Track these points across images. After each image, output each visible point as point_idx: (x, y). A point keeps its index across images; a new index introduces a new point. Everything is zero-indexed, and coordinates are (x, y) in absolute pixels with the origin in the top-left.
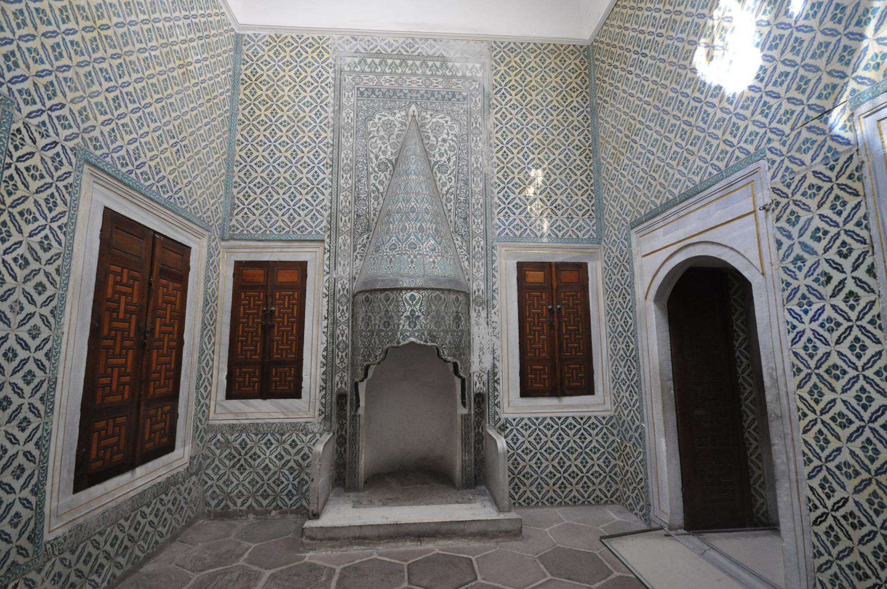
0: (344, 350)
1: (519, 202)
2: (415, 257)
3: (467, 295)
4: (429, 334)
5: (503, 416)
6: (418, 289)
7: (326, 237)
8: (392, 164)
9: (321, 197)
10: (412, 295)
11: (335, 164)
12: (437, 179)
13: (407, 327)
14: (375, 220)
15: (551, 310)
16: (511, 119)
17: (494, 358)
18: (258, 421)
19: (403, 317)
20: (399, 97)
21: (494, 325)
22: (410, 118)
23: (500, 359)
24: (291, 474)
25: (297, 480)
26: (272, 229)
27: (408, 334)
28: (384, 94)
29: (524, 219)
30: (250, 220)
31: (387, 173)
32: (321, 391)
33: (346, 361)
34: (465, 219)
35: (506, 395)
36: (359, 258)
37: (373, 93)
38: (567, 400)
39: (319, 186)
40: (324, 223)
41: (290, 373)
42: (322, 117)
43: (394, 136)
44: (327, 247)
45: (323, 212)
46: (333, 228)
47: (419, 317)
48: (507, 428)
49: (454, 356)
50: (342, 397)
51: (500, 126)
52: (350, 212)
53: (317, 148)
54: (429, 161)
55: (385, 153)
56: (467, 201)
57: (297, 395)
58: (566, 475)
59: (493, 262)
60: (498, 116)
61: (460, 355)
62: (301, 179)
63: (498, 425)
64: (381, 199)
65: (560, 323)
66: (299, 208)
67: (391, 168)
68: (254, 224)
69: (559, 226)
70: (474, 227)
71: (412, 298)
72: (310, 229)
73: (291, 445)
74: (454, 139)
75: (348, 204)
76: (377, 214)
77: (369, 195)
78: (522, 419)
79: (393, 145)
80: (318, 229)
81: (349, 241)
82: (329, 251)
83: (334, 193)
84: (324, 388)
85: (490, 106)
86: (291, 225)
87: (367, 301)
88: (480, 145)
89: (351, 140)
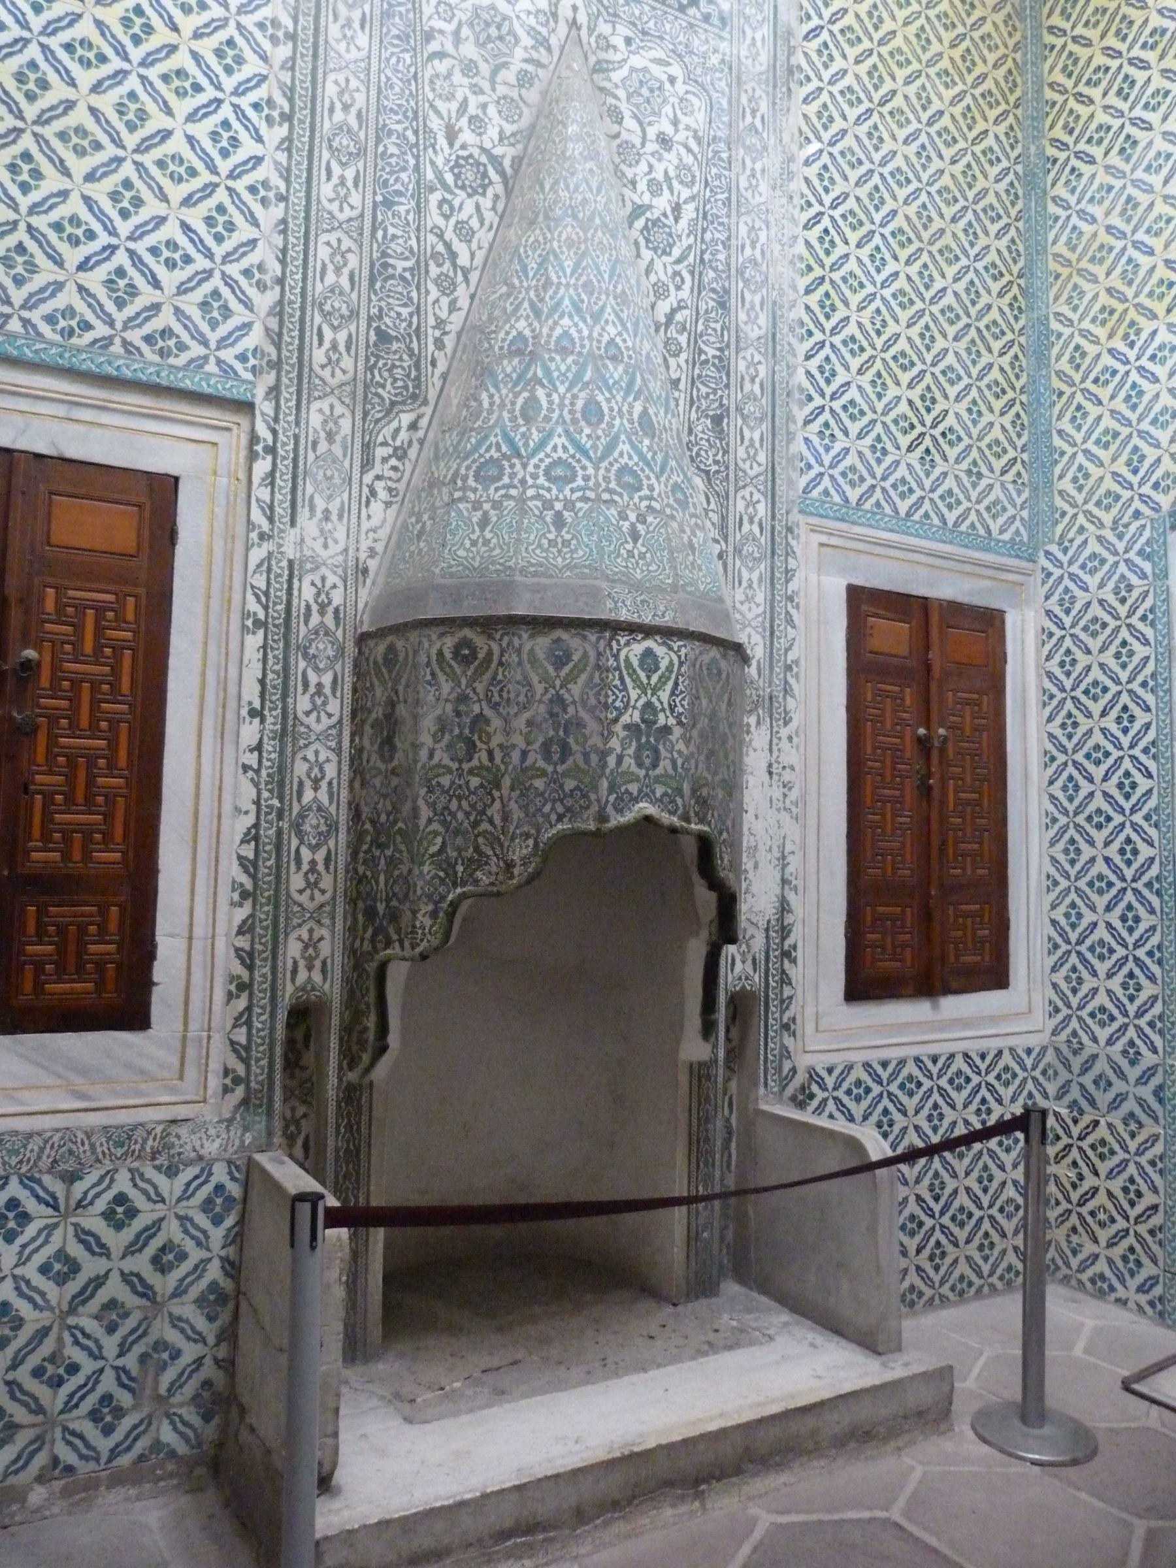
0: (323, 837)
2: (641, 519)
4: (694, 791)
5: (803, 1062)
6: (667, 633)
7: (260, 392)
8: (502, 173)
9: (245, 232)
10: (648, 653)
11: (302, 114)
13: (629, 762)
14: (442, 366)
15: (923, 744)
17: (784, 881)
19: (618, 728)
21: (787, 776)
23: (799, 883)
24: (111, 1329)
25: (138, 1350)
26: (35, 316)
27: (634, 788)
31: (486, 203)
32: (230, 996)
33: (327, 882)
34: (717, 420)
35: (810, 997)
36: (382, 494)
38: (954, 1006)
40: (254, 338)
41: (103, 928)
46: (288, 361)
47: (667, 729)
48: (812, 1096)
50: (303, 1016)
56: (723, 365)
57: (131, 1012)
59: (789, 574)
63: (790, 1091)
64: (462, 293)
65: (943, 781)
67: (499, 188)
70: (741, 453)
71: (649, 660)
72: (197, 350)
74: (693, 144)
75: (345, 282)
76: (450, 342)
80: (228, 355)
81: (346, 425)
82: (271, 450)
84: (242, 987)
85: (790, 72)
88: (763, 187)
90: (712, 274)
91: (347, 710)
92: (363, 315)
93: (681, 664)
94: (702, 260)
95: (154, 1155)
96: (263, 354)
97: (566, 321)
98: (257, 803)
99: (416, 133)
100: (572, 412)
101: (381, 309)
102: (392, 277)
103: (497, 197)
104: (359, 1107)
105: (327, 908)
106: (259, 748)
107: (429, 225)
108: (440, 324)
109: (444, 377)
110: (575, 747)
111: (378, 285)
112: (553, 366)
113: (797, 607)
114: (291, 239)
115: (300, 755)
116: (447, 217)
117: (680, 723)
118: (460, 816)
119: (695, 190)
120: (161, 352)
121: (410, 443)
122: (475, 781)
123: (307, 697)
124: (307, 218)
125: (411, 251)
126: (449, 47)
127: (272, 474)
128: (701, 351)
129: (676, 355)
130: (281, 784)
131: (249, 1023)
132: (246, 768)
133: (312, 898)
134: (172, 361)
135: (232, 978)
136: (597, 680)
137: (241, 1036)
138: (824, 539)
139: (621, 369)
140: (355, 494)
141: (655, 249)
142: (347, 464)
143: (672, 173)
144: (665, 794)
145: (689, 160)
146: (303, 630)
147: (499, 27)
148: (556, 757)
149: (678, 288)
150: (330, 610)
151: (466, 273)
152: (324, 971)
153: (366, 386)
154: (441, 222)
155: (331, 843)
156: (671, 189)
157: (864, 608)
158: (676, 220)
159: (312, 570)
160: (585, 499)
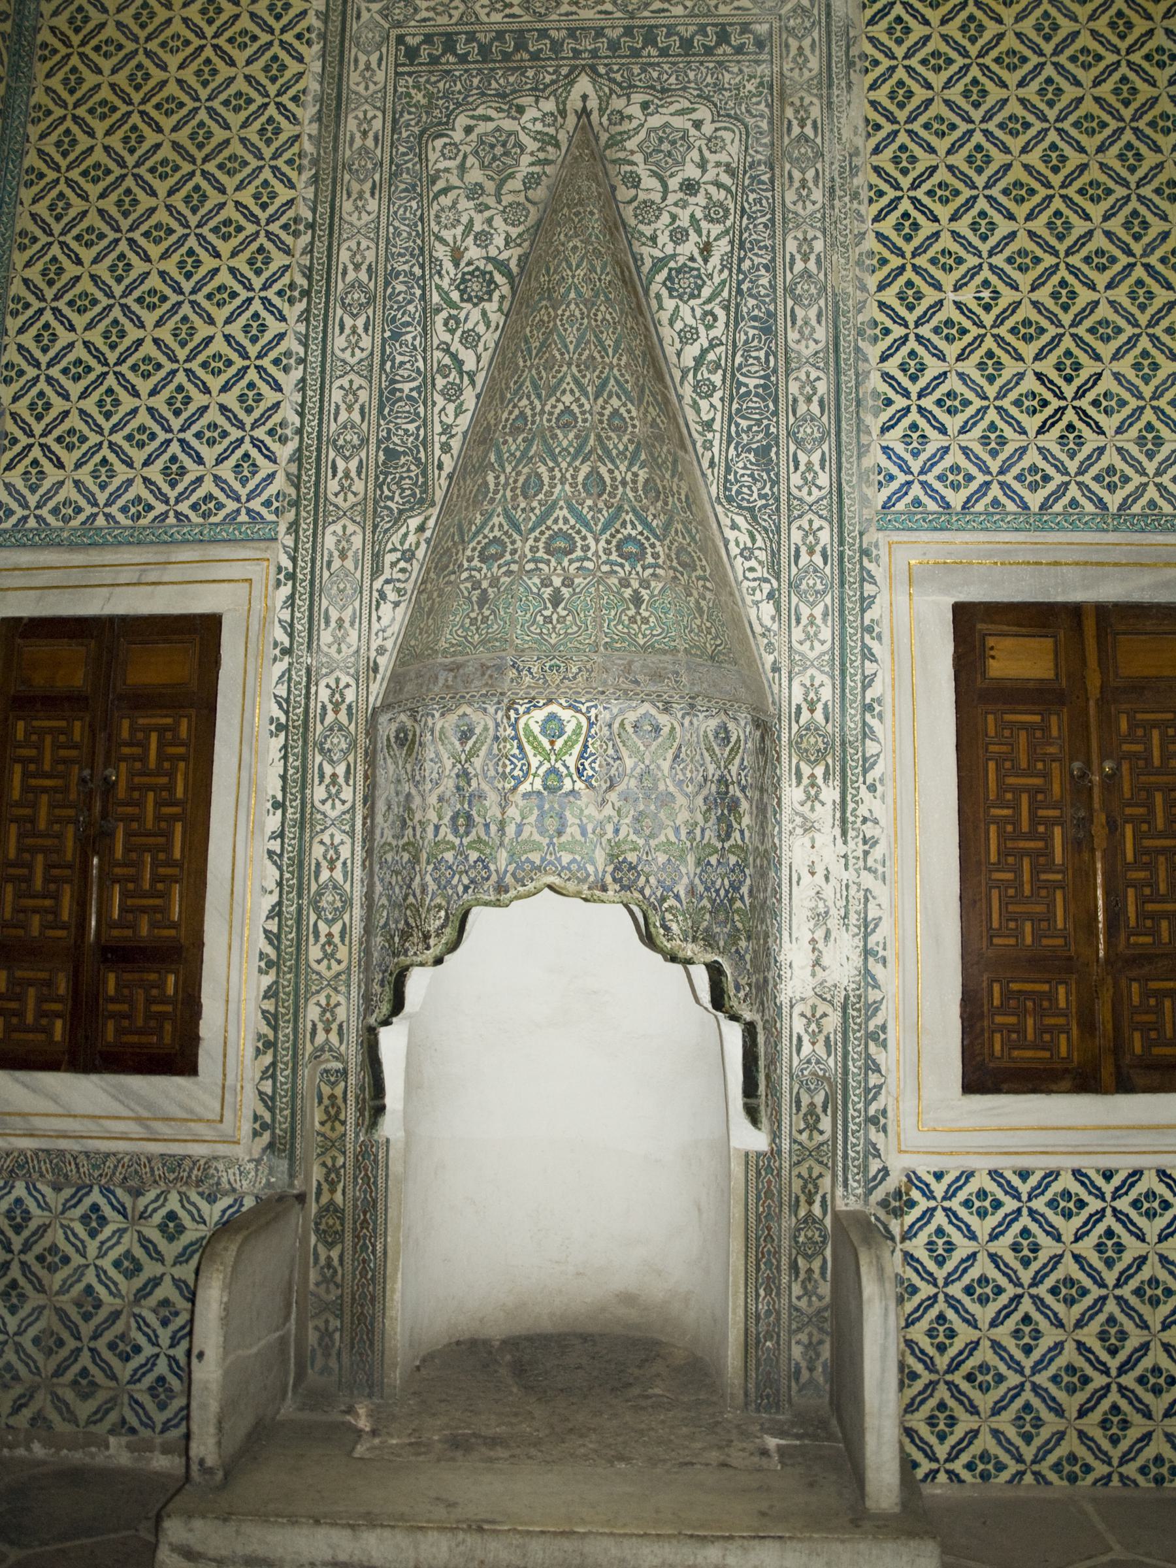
0: (338, 913)
1: (959, 388)
2: (568, 582)
4: (612, 857)
5: (898, 1164)
7: (282, 528)
8: (508, 274)
10: (552, 717)
12: (664, 317)
14: (448, 468)
16: (928, 102)
17: (867, 953)
18: (63, 1144)
19: (517, 798)
20: (535, 56)
21: (869, 830)
22: (571, 120)
23: (889, 954)
26: (114, 510)
27: (536, 858)
28: (485, 50)
29: (978, 449)
30: (47, 484)
31: (491, 307)
33: (342, 953)
34: (763, 453)
36: (392, 596)
37: (450, 47)
39: (266, 362)
40: (280, 483)
42: (283, 137)
43: (516, 184)
44: (286, 563)
45: (275, 446)
48: (912, 1204)
49: (709, 941)
51: (888, 128)
52: (364, 441)
53: (262, 239)
54: (638, 259)
55: (482, 239)
56: (769, 391)
58: (1128, 1380)
59: (866, 603)
61: (734, 937)
62: (209, 340)
63: (879, 1194)
64: (469, 398)
67: (506, 290)
68: (60, 497)
69: (1111, 470)
70: (796, 479)
72: (231, 506)
73: (163, 1228)
75: (356, 416)
76: (456, 444)
77: (427, 384)
78: (969, 1175)
79: (512, 213)
80: (255, 505)
81: (357, 541)
82: (292, 576)
84: (270, 1045)
85: (851, 64)
86: (172, 495)
87: (401, 742)
89: (372, 205)
90: (752, 302)
91: (359, 797)
92: (373, 439)
93: (591, 725)
94: (739, 292)
95: (199, 1182)
97: (525, 402)
98: (280, 884)
99: (422, 267)
103: (503, 297)
104: (376, 1161)
106: (282, 835)
107: (436, 342)
108: (447, 429)
109: (450, 477)
110: (477, 819)
112: (505, 448)
113: (879, 638)
116: (452, 332)
117: (590, 786)
119: (728, 223)
120: (204, 516)
121: (418, 544)
122: (406, 856)
124: (323, 372)
125: (418, 371)
127: (292, 597)
128: (740, 384)
129: (709, 396)
131: (273, 1077)
132: (270, 853)
133: (329, 968)
134: (213, 520)
135: (260, 1037)
137: (267, 1086)
139: (571, 436)
140: (366, 600)
142: (358, 575)
143: (699, 215)
144: (574, 861)
145: (719, 195)
146: (319, 728)
147: (504, 145)
148: (462, 830)
149: (709, 327)
150: (344, 707)
151: (471, 376)
153: (376, 502)
154: (447, 337)
155: (346, 917)
156: (699, 232)
157: (979, 626)
160: (509, 573)
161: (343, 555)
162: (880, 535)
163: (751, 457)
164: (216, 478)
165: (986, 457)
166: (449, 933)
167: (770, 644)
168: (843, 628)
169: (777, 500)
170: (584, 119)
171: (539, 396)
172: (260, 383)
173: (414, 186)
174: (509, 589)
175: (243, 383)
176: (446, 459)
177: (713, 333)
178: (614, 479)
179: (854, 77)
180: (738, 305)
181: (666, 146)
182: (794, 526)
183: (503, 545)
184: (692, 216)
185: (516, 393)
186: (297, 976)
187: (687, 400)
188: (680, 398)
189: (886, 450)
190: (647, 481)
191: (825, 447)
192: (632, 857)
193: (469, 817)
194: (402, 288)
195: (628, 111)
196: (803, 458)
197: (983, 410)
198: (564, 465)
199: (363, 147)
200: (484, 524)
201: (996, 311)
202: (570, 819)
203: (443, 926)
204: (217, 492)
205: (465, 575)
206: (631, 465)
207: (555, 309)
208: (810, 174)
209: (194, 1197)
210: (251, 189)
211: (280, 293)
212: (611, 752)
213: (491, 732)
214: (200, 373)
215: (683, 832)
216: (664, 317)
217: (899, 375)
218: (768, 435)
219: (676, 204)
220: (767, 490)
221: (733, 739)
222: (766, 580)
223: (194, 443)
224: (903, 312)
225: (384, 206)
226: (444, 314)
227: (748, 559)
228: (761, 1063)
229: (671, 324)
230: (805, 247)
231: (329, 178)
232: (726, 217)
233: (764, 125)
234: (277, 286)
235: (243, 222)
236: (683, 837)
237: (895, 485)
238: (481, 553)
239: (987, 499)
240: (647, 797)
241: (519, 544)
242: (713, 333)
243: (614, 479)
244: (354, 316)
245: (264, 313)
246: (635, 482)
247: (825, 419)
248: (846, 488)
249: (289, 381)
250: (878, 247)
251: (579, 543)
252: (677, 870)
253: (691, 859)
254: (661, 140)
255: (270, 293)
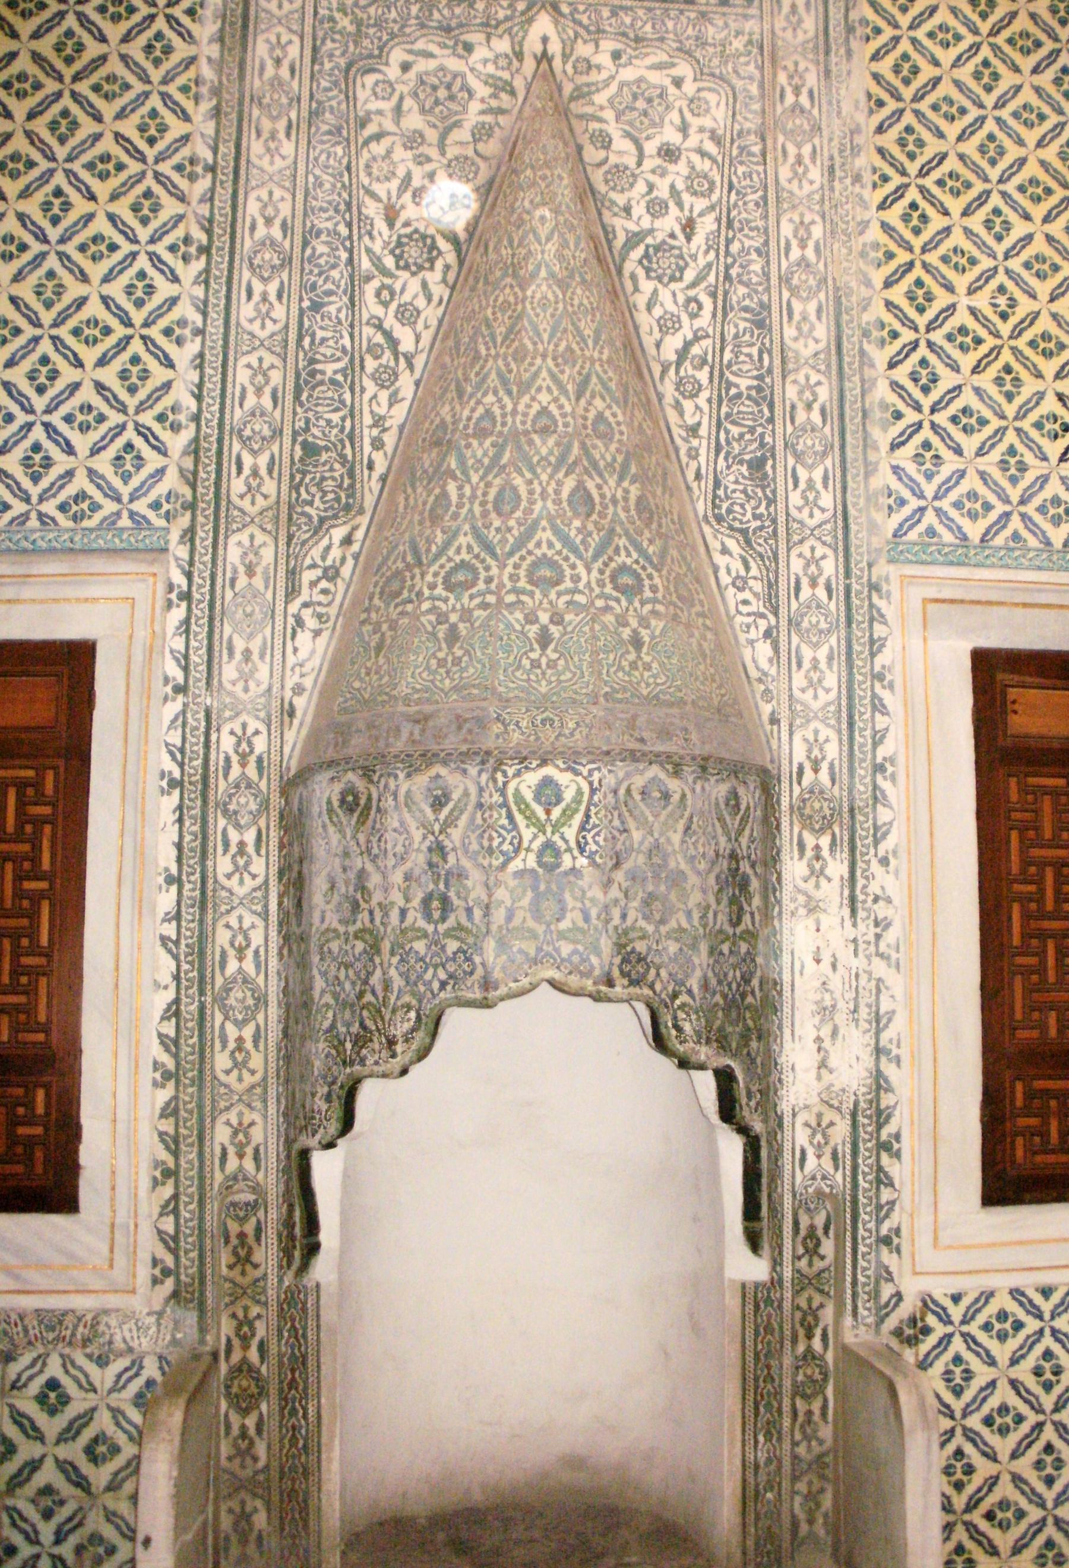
1: (975, 404)
2: (557, 619)
3: (768, 783)
4: (620, 946)
7: (174, 536)
10: (547, 782)
11: (222, 241)
12: (641, 300)
14: (380, 468)
17: (878, 1051)
21: (881, 910)
23: (904, 1052)
31: (433, 278)
33: (256, 1061)
34: (757, 465)
36: (311, 623)
39: (154, 332)
40: (171, 481)
43: (463, 134)
45: (165, 435)
49: (722, 1043)
53: (149, 181)
54: (609, 233)
56: (763, 395)
59: (875, 646)
60: (885, 67)
61: (745, 1038)
62: (81, 302)
64: (406, 384)
66: (68, 419)
67: (451, 258)
70: (795, 499)
72: (110, 507)
74: (710, 147)
75: (267, 402)
76: (390, 440)
77: (354, 366)
78: (988, 1296)
80: (141, 506)
82: (186, 596)
83: (213, 359)
90: (742, 290)
91: (274, 870)
92: (288, 431)
93: (593, 791)
94: (727, 277)
96: (177, 497)
97: (490, 398)
99: (349, 225)
100: (483, 504)
101: (307, 421)
102: (322, 383)
103: (447, 267)
105: (258, 1090)
107: (365, 316)
108: (379, 421)
109: (383, 479)
110: (456, 902)
111: (304, 396)
112: (469, 453)
113: (891, 686)
114: (208, 371)
115: (221, 922)
116: (386, 304)
118: (348, 986)
119: (715, 197)
120: (75, 518)
121: (343, 560)
122: (360, 946)
123: (228, 857)
125: (344, 350)
126: (389, 125)
127: (187, 621)
128: (730, 385)
129: (694, 396)
130: (202, 954)
132: (164, 940)
133: (240, 1079)
134: (86, 523)
136: (479, 821)
138: (932, 593)
140: (279, 627)
141: (659, 279)
142: (269, 596)
143: (680, 185)
144: (575, 952)
146: (222, 785)
147: (449, 87)
148: (436, 915)
149: (693, 316)
150: (253, 759)
151: (409, 359)
152: (256, 1158)
153: (291, 507)
154: (379, 311)
155: (260, 1018)
156: (680, 205)
157: (1000, 676)
158: (689, 239)
159: (231, 719)
160: (484, 606)
161: (250, 572)
162: (891, 568)
163: (744, 469)
164: (91, 472)
165: (1005, 483)
166: (420, 1036)
167: (767, 691)
168: (850, 674)
169: (774, 521)
170: (544, 65)
171: (509, 393)
172: (146, 357)
173: (339, 130)
174: (485, 625)
175: (125, 356)
176: (379, 458)
177: (698, 323)
178: (603, 496)
179: (854, 44)
180: (726, 293)
181: (641, 104)
182: (794, 553)
183: (474, 570)
184: (672, 187)
185: (478, 387)
186: (201, 1089)
187: (669, 400)
188: (660, 397)
189: (896, 470)
190: (639, 500)
191: (828, 462)
192: (641, 947)
193: (445, 900)
194: (325, 249)
195: (597, 59)
196: (803, 474)
197: (1001, 432)
198: (544, 477)
199: (276, 77)
200: (447, 545)
201: (1013, 320)
202: (570, 902)
203: (413, 1030)
204: (91, 490)
205: (426, 606)
206: (621, 479)
207: (523, 289)
208: (807, 150)
209: (80, 1359)
210: (135, 119)
211: (173, 248)
212: (616, 823)
213: (473, 798)
214: (70, 341)
215: (696, 915)
216: (641, 300)
217: (909, 385)
218: (762, 445)
219: (653, 172)
220: (762, 510)
221: (743, 807)
222: (762, 616)
223: (62, 427)
224: (912, 313)
225: (302, 150)
226: (375, 283)
227: (741, 589)
228: (764, 1181)
229: (649, 308)
230: (802, 232)
231: (233, 114)
232: (711, 190)
233: (754, 89)
234: (168, 240)
235: (125, 158)
236: (696, 923)
237: (906, 511)
238: (446, 580)
239: (1007, 532)
240: (656, 877)
241: (495, 571)
242: (698, 323)
243: (603, 496)
244: (265, 280)
245: (151, 272)
246: (626, 499)
247: (827, 430)
248: (852, 512)
249: (183, 355)
250: (883, 239)
251: (568, 572)
252: (689, 960)
253: (704, 947)
254: (635, 97)
255: (160, 248)
